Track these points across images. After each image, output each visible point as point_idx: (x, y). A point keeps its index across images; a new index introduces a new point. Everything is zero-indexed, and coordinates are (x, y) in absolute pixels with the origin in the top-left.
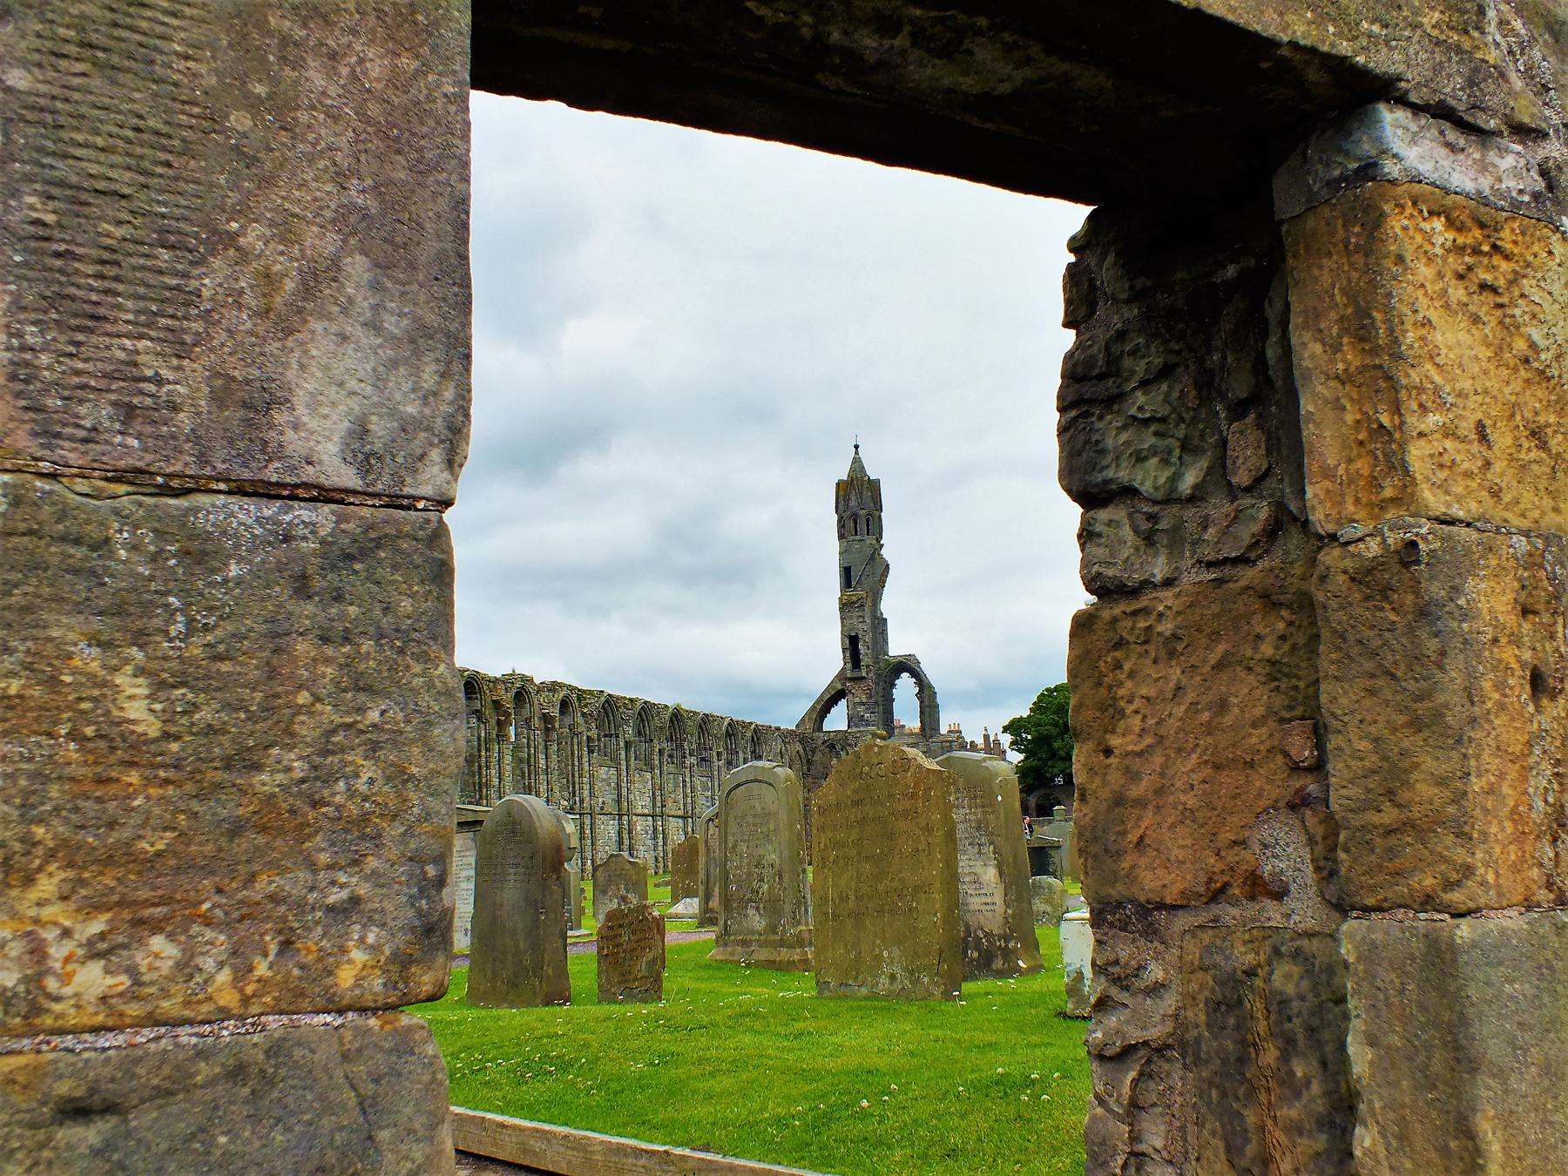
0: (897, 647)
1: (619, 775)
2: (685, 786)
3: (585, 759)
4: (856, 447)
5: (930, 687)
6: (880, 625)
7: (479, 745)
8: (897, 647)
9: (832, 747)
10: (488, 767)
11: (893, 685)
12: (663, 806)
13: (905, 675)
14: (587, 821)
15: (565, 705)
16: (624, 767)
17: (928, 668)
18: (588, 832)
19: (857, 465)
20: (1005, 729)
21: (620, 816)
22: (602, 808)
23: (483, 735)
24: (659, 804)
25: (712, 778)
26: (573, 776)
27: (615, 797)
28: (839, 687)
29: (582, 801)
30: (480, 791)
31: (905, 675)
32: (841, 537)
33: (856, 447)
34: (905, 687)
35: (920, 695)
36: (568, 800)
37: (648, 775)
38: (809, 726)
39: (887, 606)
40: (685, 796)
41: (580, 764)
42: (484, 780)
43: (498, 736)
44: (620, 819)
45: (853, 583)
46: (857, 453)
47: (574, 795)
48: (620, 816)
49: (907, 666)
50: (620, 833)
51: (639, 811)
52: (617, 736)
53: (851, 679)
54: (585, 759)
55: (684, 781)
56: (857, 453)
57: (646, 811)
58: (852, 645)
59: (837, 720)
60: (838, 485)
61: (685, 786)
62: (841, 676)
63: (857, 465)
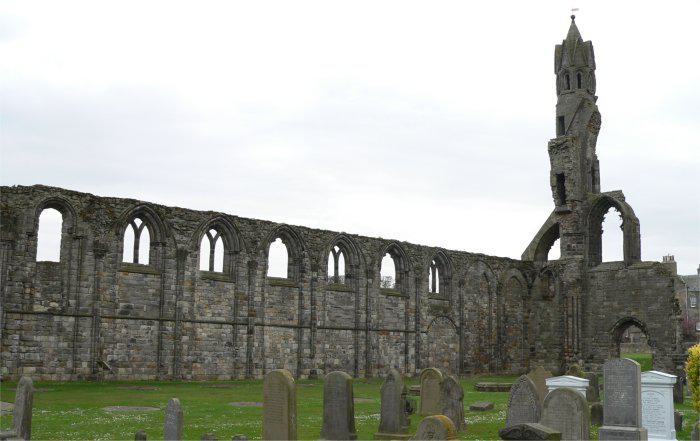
0: (606, 186)
4: (573, 17)
6: (592, 169)
8: (606, 186)
9: (549, 273)
11: (602, 219)
13: (612, 210)
19: (574, 32)
25: (357, 292)
31: (612, 210)
32: (559, 93)
33: (573, 17)
34: (612, 220)
40: (302, 307)
46: (573, 22)
49: (615, 200)
55: (301, 294)
56: (573, 22)
58: (559, 182)
59: (555, 253)
60: (557, 47)
62: (557, 213)
63: (574, 32)
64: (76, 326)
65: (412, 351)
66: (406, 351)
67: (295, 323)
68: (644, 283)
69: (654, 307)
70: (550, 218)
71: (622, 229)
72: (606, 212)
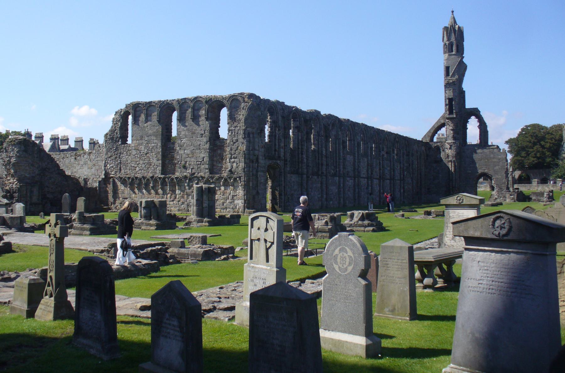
0: (469, 105)
1: (354, 159)
2: (380, 165)
3: (341, 151)
4: (453, 12)
5: (485, 124)
6: (461, 95)
7: (298, 143)
8: (469, 105)
10: (302, 154)
12: (372, 174)
13: (473, 118)
14: (342, 180)
15: (333, 125)
16: (356, 155)
17: (483, 114)
18: (342, 185)
20: (507, 142)
21: (355, 178)
22: (348, 174)
23: (300, 138)
24: (370, 173)
26: (336, 158)
27: (353, 169)
28: (442, 121)
29: (340, 171)
30: (299, 165)
31: (473, 118)
33: (453, 12)
35: (480, 127)
36: (334, 170)
37: (366, 160)
38: (428, 140)
39: (465, 86)
40: (380, 169)
41: (339, 153)
42: (300, 160)
43: (306, 139)
44: (354, 180)
45: (451, 74)
47: (336, 168)
48: (355, 178)
49: (475, 112)
50: (354, 186)
51: (362, 176)
52: (354, 141)
53: (448, 119)
54: (341, 151)
55: (380, 163)
57: (364, 176)
58: (450, 103)
61: (380, 165)
64: (339, 182)
65: (402, 191)
66: (400, 191)
67: (378, 177)
68: (492, 156)
69: (497, 168)
70: (439, 120)
71: (479, 128)
72: (470, 118)
